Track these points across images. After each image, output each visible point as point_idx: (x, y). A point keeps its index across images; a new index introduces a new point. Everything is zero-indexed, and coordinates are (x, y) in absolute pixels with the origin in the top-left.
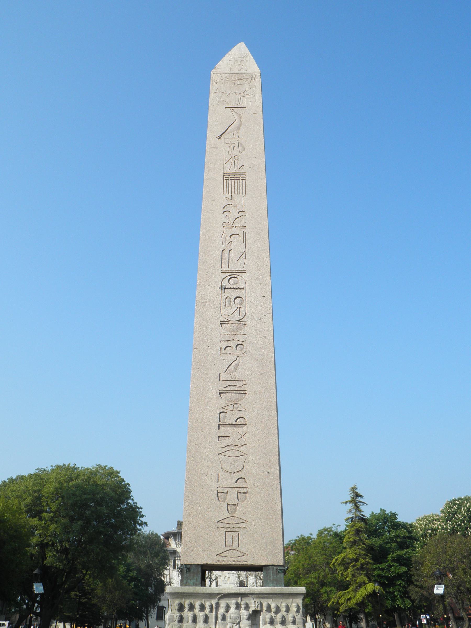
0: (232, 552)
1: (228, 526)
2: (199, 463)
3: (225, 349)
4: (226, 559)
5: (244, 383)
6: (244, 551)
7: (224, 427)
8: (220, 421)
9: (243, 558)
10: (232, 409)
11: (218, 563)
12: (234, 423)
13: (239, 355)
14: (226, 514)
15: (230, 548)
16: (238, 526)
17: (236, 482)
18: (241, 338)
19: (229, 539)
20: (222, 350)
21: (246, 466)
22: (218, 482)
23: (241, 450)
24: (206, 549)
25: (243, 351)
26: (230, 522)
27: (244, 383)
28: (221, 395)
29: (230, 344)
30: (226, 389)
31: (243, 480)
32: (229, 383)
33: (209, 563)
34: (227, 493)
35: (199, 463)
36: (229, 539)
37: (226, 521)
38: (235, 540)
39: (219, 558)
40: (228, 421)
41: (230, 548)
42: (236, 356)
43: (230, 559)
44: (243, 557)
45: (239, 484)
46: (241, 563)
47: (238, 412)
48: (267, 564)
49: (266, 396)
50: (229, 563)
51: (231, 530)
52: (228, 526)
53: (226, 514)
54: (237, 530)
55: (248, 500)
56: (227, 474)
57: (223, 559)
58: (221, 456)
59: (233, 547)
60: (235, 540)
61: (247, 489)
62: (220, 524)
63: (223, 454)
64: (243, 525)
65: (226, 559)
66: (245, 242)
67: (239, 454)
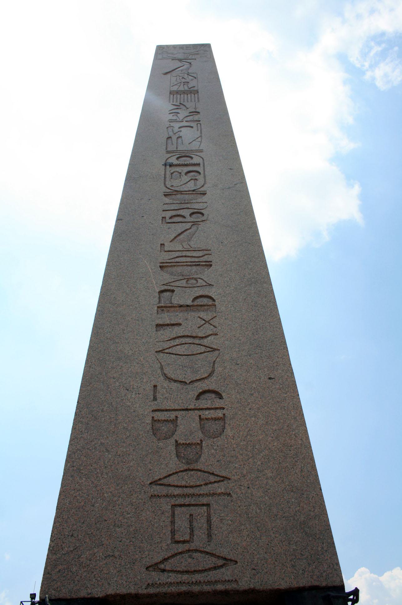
0: (190, 557)
1: (177, 491)
2: (113, 368)
3: (171, 218)
4: (173, 578)
5: (207, 252)
6: (224, 552)
7: (168, 311)
8: (159, 302)
9: (226, 573)
10: (185, 285)
11: (151, 591)
12: (189, 302)
13: (194, 223)
14: (174, 464)
15: (186, 547)
16: (204, 490)
17: (198, 397)
18: (196, 206)
19: (182, 523)
20: (167, 218)
21: (219, 369)
22: (155, 399)
23: (205, 344)
24: (117, 554)
25: (203, 218)
26: (184, 483)
27: (207, 252)
28: (165, 269)
29: (181, 212)
30: (173, 260)
31: (213, 396)
32: (177, 254)
33: (123, 591)
34: (174, 421)
35: (113, 368)
36: (182, 523)
37: (171, 480)
38: (201, 523)
39: (156, 577)
40: (176, 300)
41: (186, 547)
42: (190, 224)
43: (185, 577)
44: (223, 570)
45: (205, 402)
46: (220, 587)
47: (196, 289)
48: (295, 585)
49: (250, 267)
50: (184, 588)
51: (187, 501)
52: (177, 491)
53: (174, 464)
54: (205, 500)
55: (229, 431)
56: (174, 385)
57: (164, 578)
58: (162, 355)
59: (193, 546)
60: (201, 523)
61: (224, 411)
62: (157, 490)
63: (166, 351)
64: (220, 488)
65: (173, 578)
66: (199, 129)
67: (203, 349)
